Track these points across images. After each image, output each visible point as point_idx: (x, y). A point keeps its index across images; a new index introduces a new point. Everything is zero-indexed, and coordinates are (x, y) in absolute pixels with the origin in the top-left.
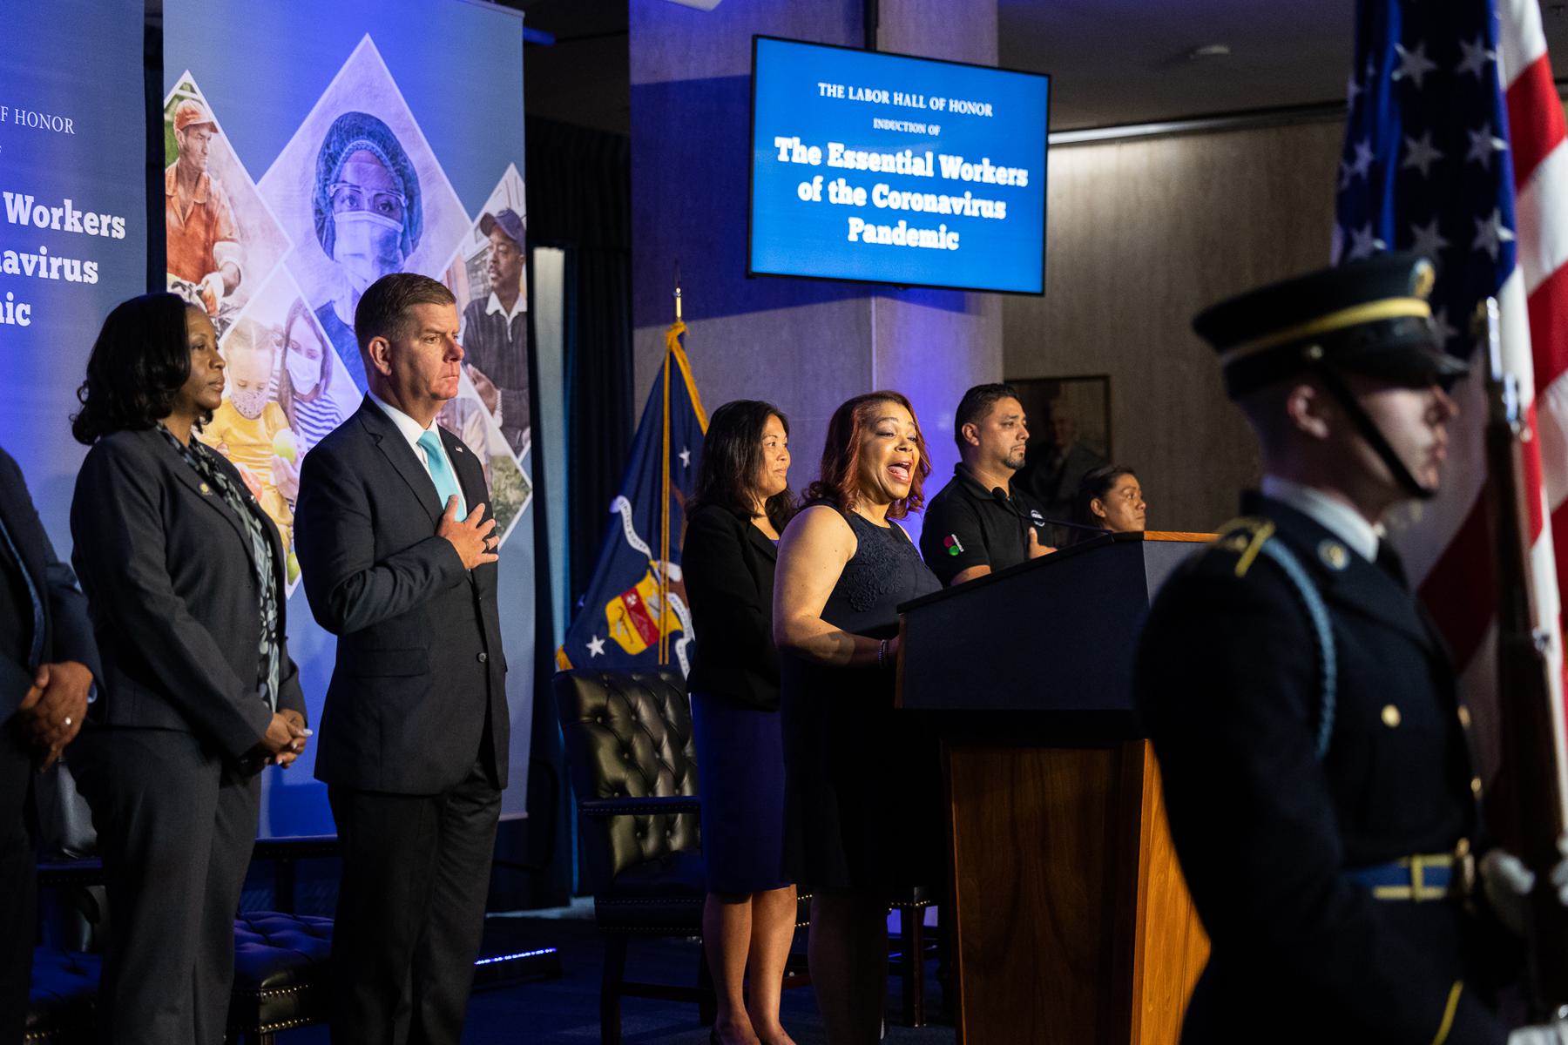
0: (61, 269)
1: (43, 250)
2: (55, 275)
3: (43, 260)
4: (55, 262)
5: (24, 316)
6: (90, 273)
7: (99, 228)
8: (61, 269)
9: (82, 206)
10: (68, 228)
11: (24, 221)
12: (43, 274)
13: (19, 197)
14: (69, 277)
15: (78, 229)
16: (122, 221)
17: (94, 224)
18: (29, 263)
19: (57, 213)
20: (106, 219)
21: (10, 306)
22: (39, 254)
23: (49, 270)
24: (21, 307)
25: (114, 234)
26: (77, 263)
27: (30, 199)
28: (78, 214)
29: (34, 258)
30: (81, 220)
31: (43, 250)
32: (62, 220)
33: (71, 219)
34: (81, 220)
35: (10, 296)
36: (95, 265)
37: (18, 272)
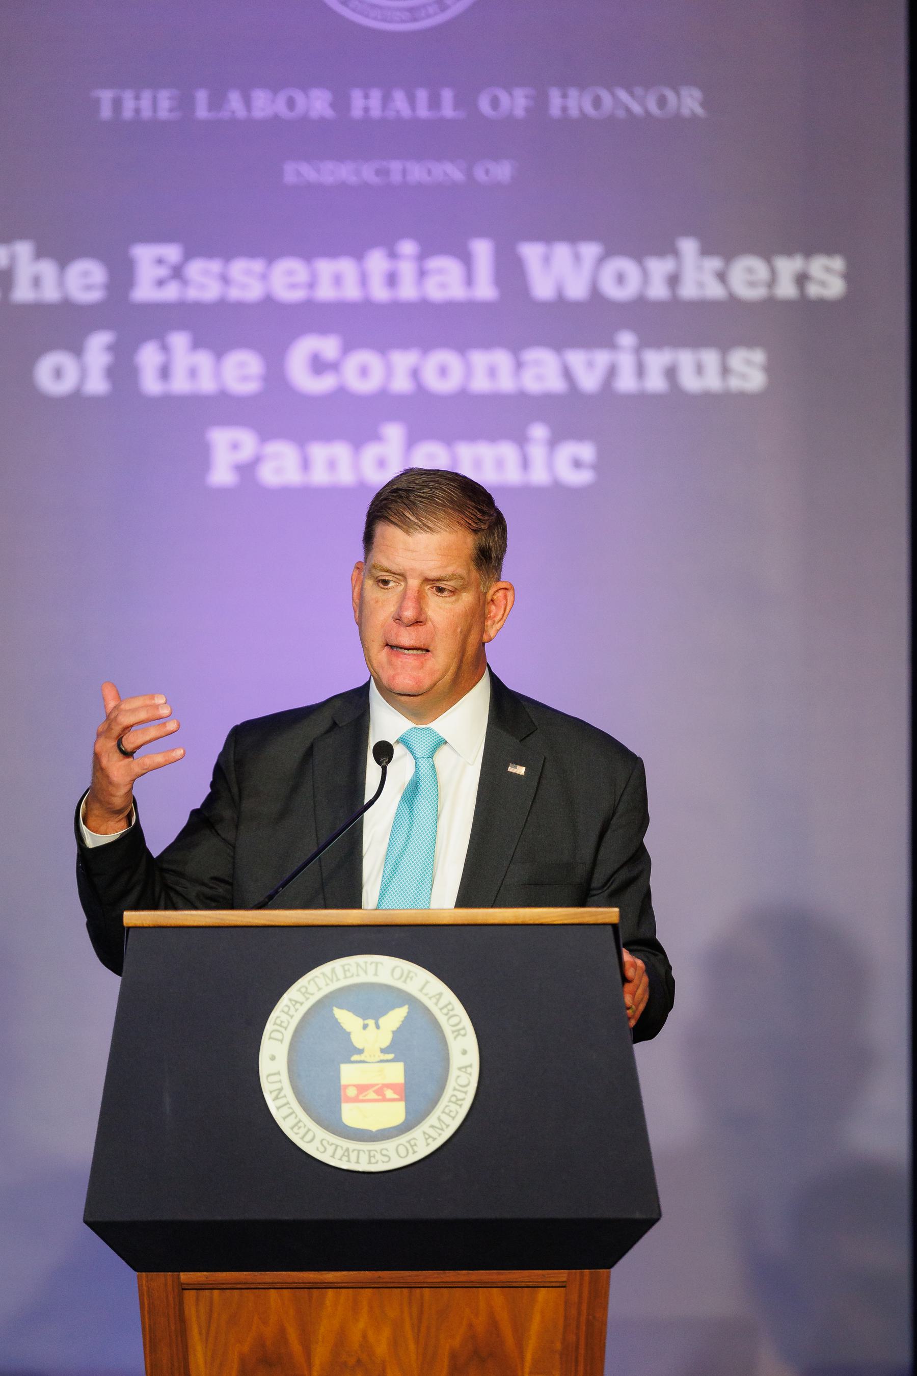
0: (671, 373)
1: (627, 339)
2: (656, 383)
3: (626, 362)
4: (656, 360)
5: (577, 464)
6: (749, 370)
7: (773, 281)
8: (671, 373)
9: (722, 246)
10: (688, 291)
11: (577, 290)
12: (626, 383)
13: (562, 251)
14: (690, 382)
15: (715, 291)
16: (838, 263)
17: (748, 277)
18: (588, 368)
19: (659, 268)
20: (788, 267)
21: (537, 452)
22: (611, 345)
23: (641, 371)
24: (568, 450)
25: (813, 290)
26: (711, 358)
27: (590, 250)
28: (714, 263)
29: (602, 358)
30: (722, 277)
31: (627, 339)
32: (674, 280)
33: (698, 275)
34: (722, 277)
35: (539, 432)
36: (758, 356)
37: (555, 384)
